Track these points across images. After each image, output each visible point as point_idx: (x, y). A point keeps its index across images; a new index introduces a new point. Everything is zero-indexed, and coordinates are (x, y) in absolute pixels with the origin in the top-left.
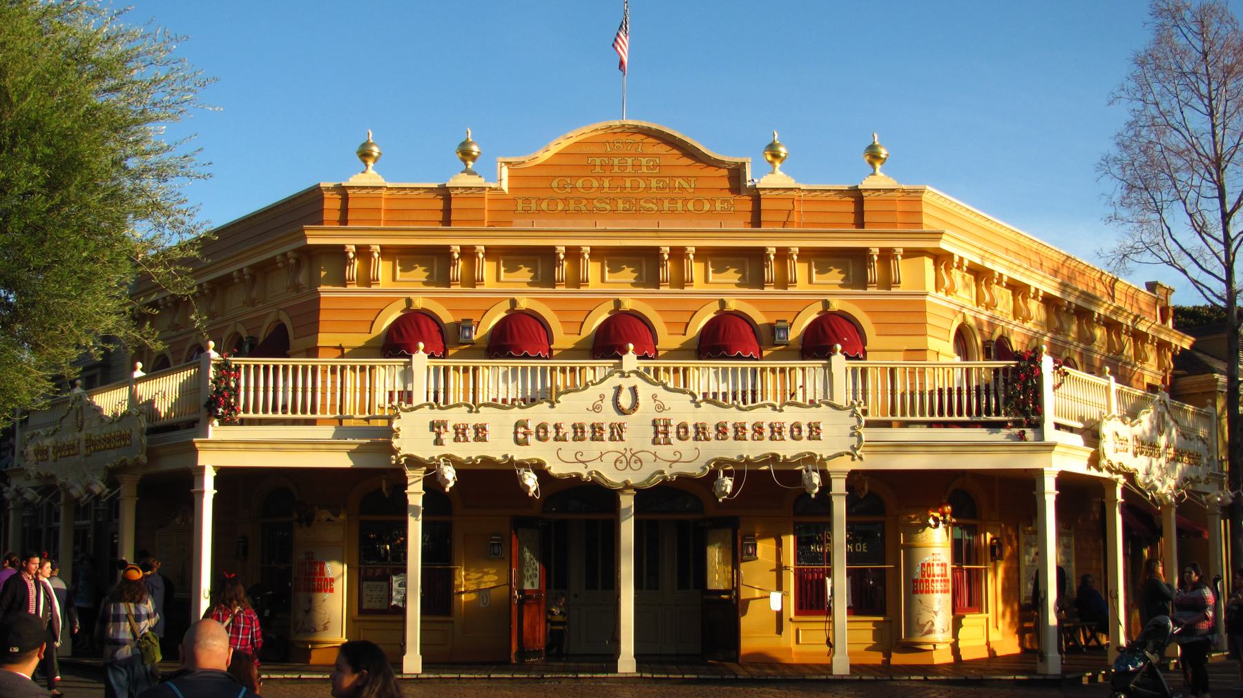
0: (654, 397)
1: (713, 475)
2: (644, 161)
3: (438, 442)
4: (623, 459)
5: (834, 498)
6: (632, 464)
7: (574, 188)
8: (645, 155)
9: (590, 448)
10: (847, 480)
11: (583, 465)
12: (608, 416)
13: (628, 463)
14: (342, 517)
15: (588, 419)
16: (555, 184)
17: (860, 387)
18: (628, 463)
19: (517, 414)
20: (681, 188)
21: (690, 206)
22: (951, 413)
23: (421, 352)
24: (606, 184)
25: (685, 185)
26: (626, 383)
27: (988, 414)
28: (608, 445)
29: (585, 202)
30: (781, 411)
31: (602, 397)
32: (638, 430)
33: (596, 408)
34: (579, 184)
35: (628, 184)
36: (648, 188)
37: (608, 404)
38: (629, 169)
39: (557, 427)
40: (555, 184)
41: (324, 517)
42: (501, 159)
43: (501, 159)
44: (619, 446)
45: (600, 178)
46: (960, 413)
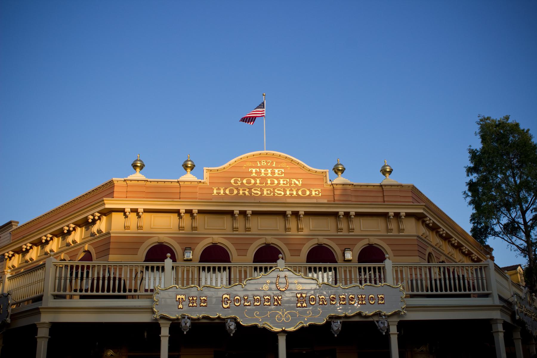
1: (328, 324)
2: (276, 171)
5: (392, 336)
7: (242, 183)
8: (276, 168)
10: (397, 326)
16: (232, 181)
17: (399, 276)
20: (295, 184)
22: (446, 290)
23: (169, 258)
24: (258, 182)
25: (297, 182)
26: (282, 274)
34: (245, 181)
35: (269, 182)
36: (279, 183)
41: (109, 354)
42: (207, 168)
43: (205, 168)
45: (254, 178)
46: (451, 290)
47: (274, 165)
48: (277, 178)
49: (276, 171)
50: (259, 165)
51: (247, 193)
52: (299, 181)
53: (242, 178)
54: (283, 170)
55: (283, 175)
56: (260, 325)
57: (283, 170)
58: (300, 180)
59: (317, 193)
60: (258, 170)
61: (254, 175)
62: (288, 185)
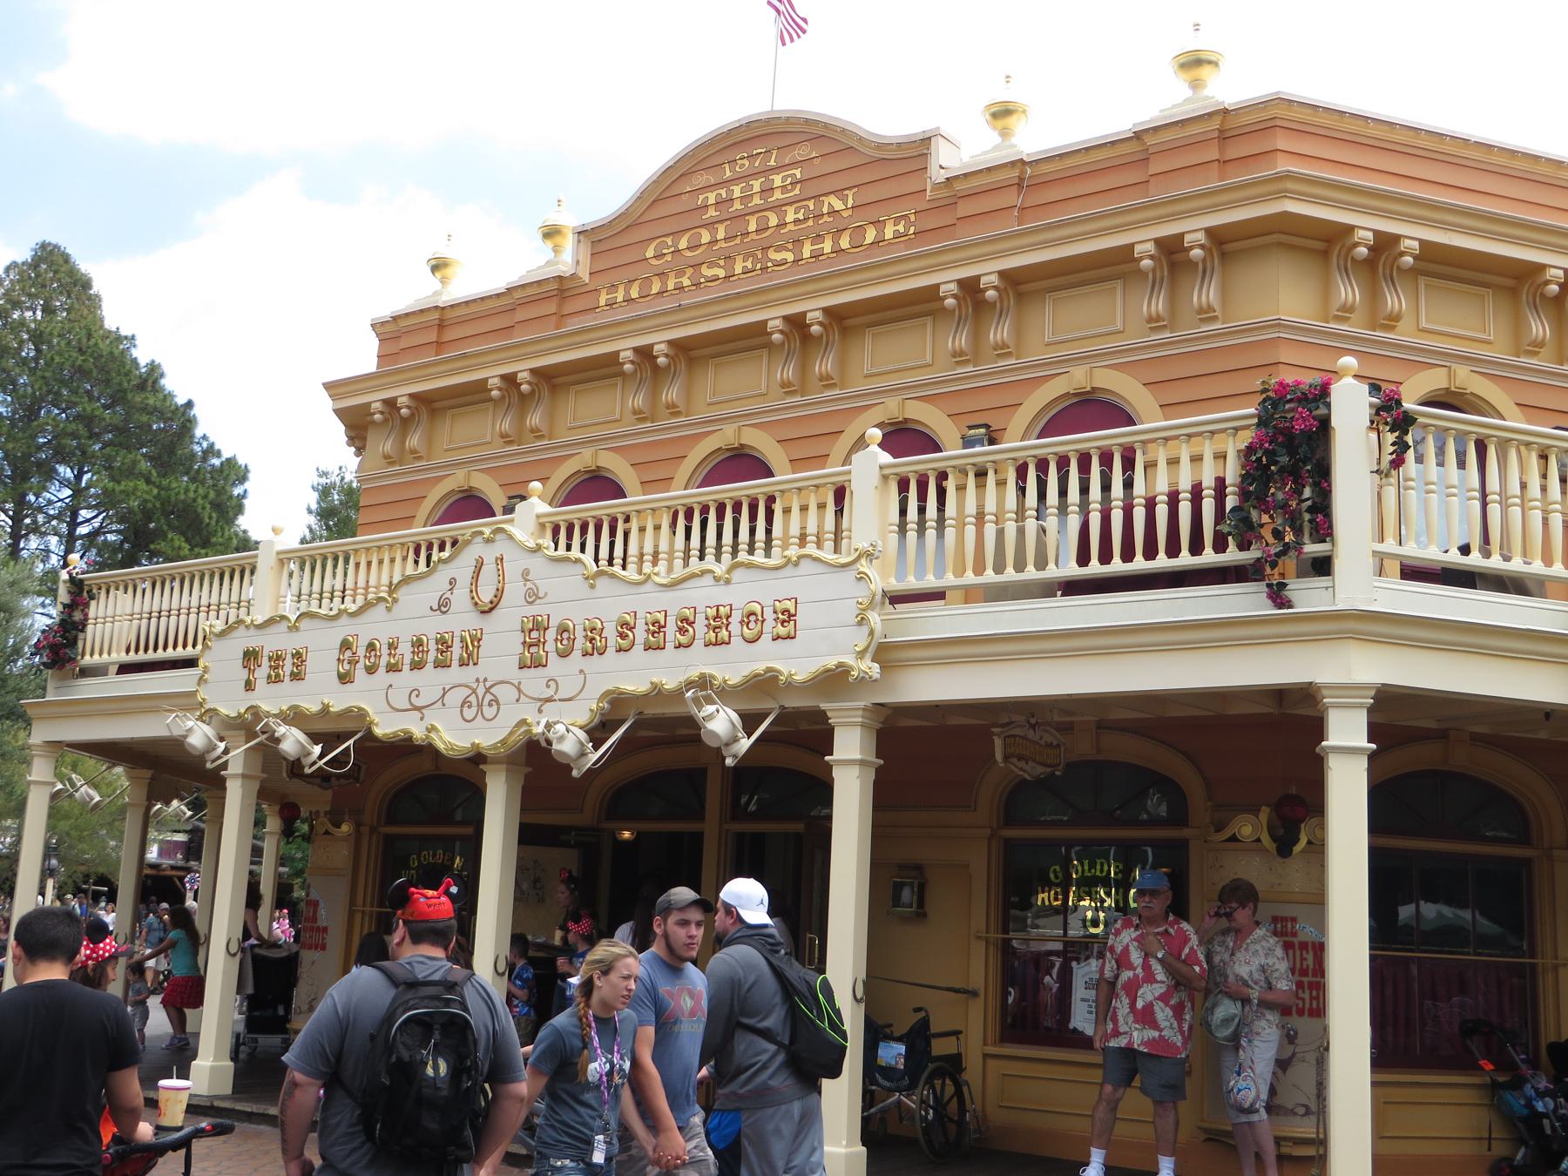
0: (525, 575)
2: (777, 180)
3: (249, 686)
4: (473, 699)
6: (486, 709)
9: (430, 681)
11: (417, 714)
12: (461, 620)
13: (480, 706)
14: (345, 828)
15: (432, 627)
18: (480, 706)
19: (343, 629)
20: (833, 212)
21: (845, 243)
25: (838, 205)
27: (1220, 546)
28: (455, 674)
29: (689, 271)
30: (728, 582)
31: (453, 582)
32: (502, 643)
33: (443, 606)
37: (460, 598)
38: (757, 200)
39: (391, 646)
40: (650, 253)
44: (469, 674)
47: (772, 163)
48: (778, 207)
49: (777, 180)
50: (728, 173)
51: (686, 282)
52: (844, 200)
53: (677, 234)
54: (798, 173)
55: (797, 191)
56: (418, 733)
57: (798, 173)
58: (850, 193)
59: (901, 228)
60: (723, 193)
61: (712, 212)
62: (810, 223)
